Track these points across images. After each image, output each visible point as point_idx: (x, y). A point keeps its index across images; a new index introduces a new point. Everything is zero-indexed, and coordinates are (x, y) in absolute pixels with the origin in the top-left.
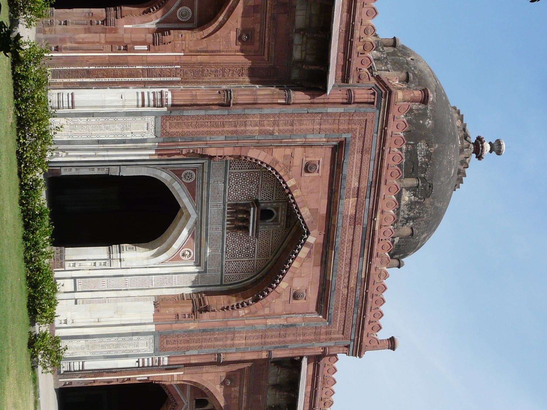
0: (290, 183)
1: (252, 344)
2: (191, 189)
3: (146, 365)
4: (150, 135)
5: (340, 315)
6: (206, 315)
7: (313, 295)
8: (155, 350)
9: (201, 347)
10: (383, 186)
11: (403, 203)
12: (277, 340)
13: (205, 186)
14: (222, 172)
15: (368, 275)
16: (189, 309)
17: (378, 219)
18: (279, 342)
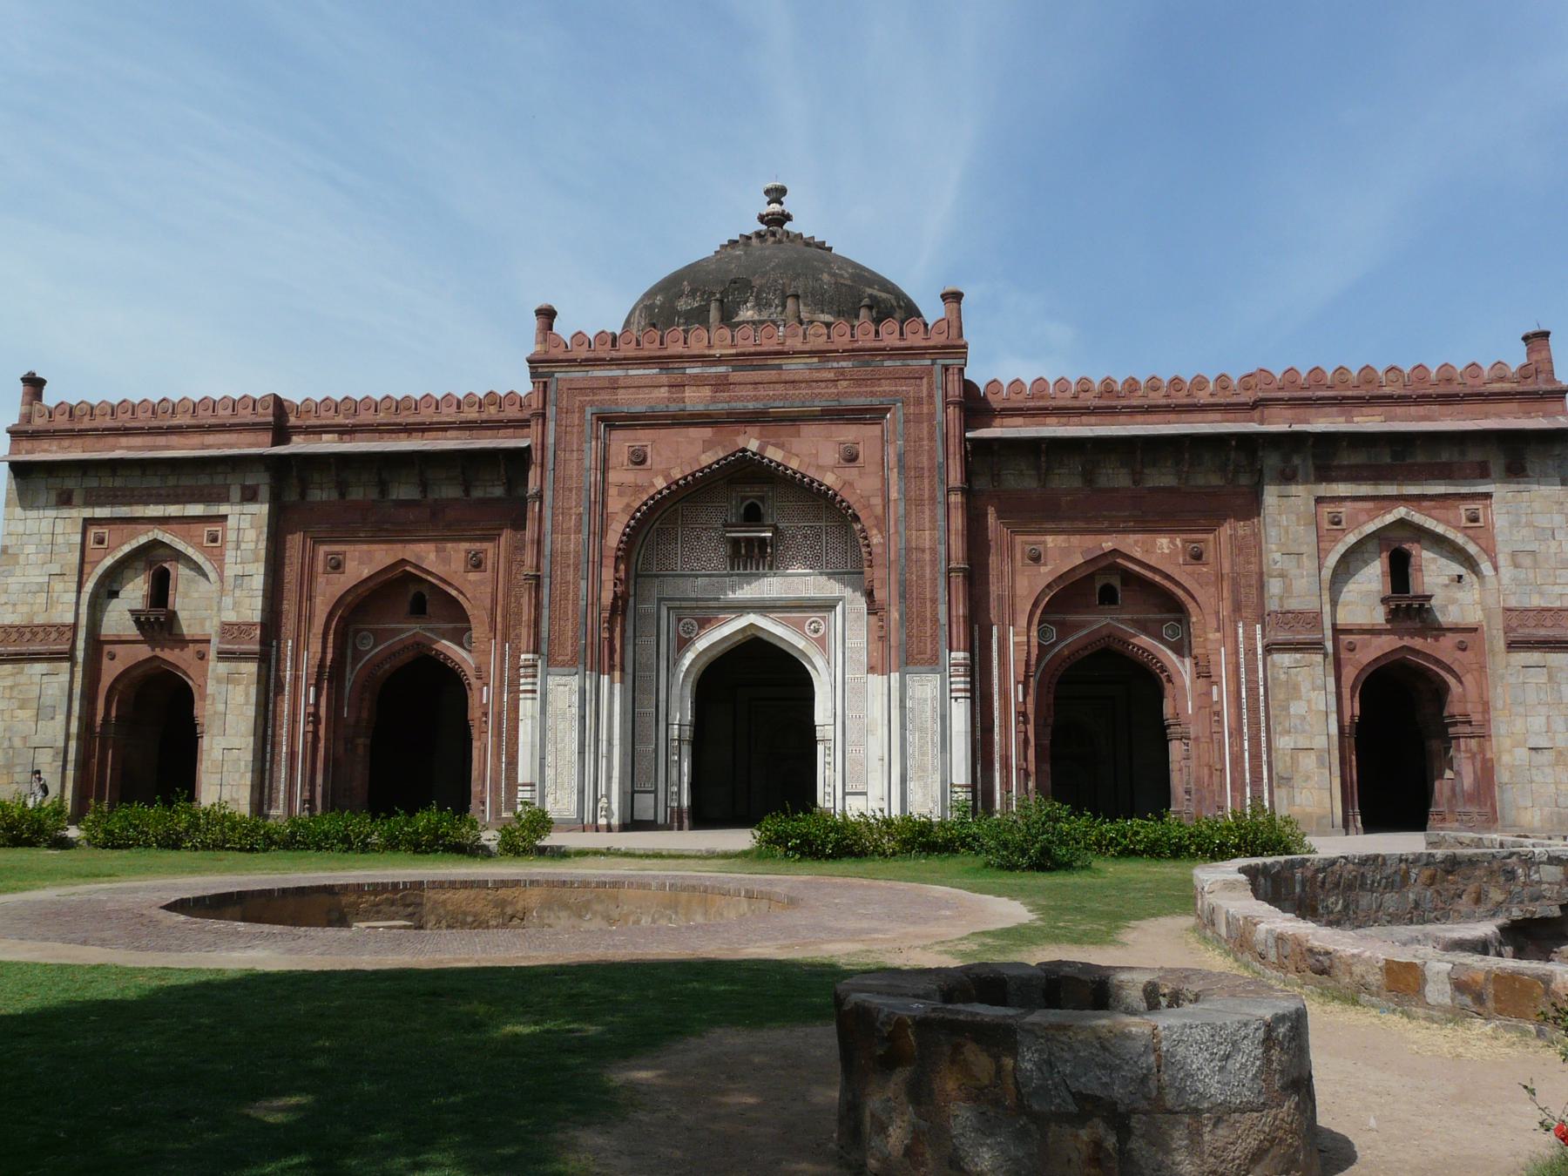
0: (660, 483)
1: (933, 519)
2: (704, 623)
3: (962, 686)
4: (575, 682)
5: (886, 387)
6: (879, 595)
7: (849, 433)
8: (933, 672)
9: (934, 601)
10: (669, 352)
11: (756, 317)
12: (926, 481)
13: (701, 604)
14: (680, 581)
15: (812, 353)
16: (874, 619)
17: (717, 352)
18: (931, 478)
